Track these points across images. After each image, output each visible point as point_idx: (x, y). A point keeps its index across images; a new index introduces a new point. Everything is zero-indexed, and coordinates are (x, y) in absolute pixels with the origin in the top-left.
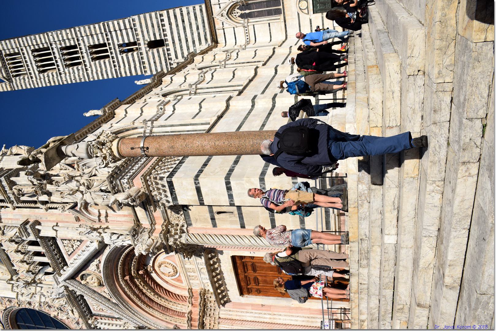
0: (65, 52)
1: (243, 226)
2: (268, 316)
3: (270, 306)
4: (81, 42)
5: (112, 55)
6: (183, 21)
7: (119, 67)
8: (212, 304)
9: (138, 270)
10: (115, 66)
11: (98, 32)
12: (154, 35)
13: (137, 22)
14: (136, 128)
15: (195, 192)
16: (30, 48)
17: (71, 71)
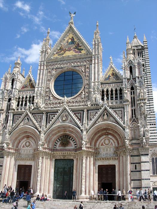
1: (132, 171)
9: (108, 133)
15: (145, 161)
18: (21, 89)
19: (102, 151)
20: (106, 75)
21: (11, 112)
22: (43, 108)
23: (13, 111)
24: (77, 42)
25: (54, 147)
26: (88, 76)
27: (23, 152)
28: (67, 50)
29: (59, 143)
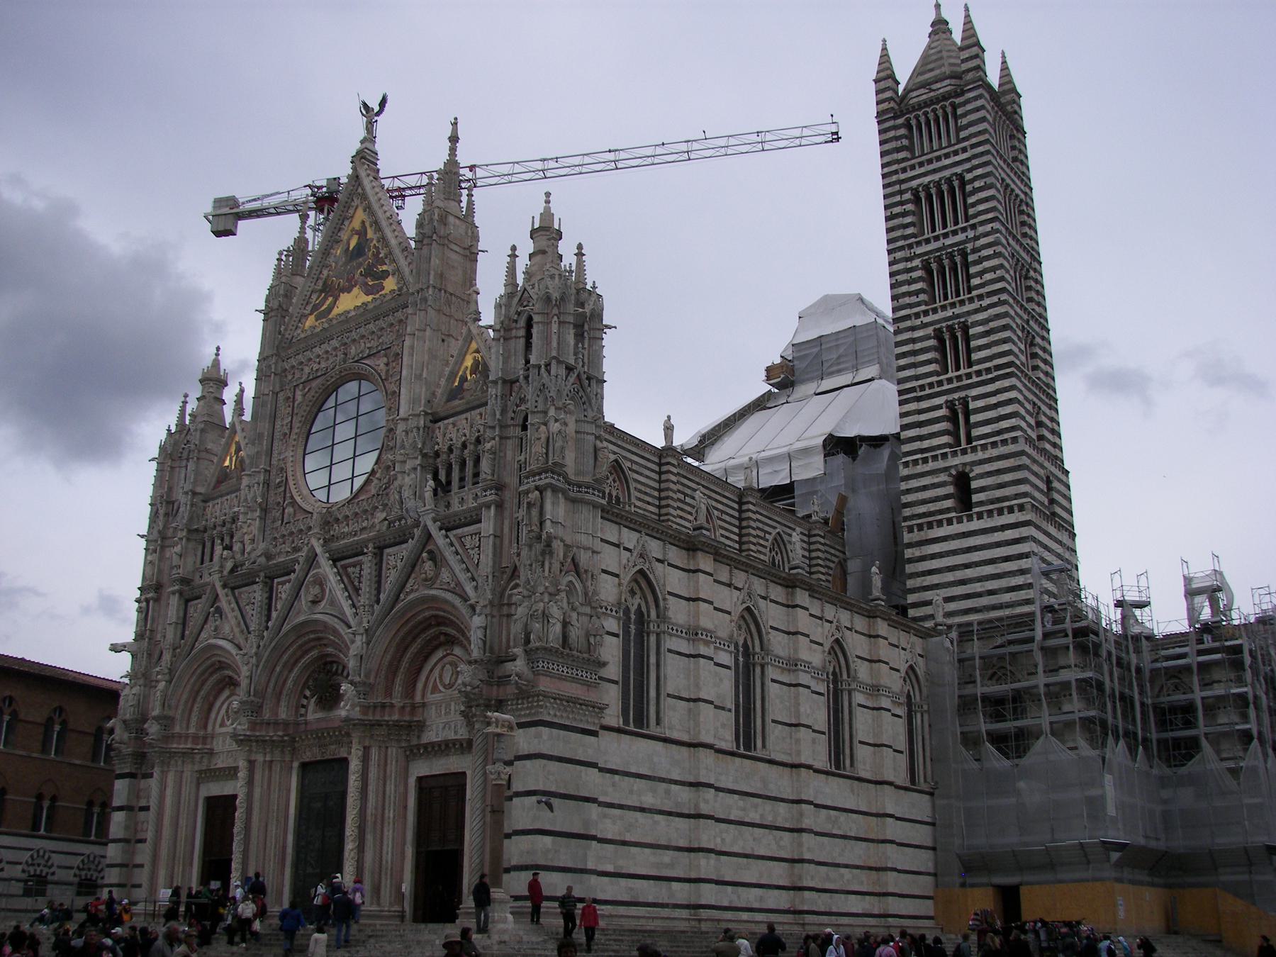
0: (958, 259)
2: (391, 816)
3: (405, 817)
4: (976, 305)
5: (945, 383)
6: (1007, 559)
7: (919, 399)
8: (404, 738)
9: (445, 634)
10: (922, 388)
11: (995, 350)
12: (982, 489)
13: (1011, 448)
14: (657, 606)
15: (526, 753)
16: (969, 171)
17: (915, 275)
18: (214, 489)
19: (433, 717)
20: (453, 375)
21: (173, 593)
22: (263, 560)
23: (177, 587)
24: (375, 242)
25: (302, 715)
26: (394, 392)
27: (220, 742)
28: (343, 290)
29: (313, 700)
